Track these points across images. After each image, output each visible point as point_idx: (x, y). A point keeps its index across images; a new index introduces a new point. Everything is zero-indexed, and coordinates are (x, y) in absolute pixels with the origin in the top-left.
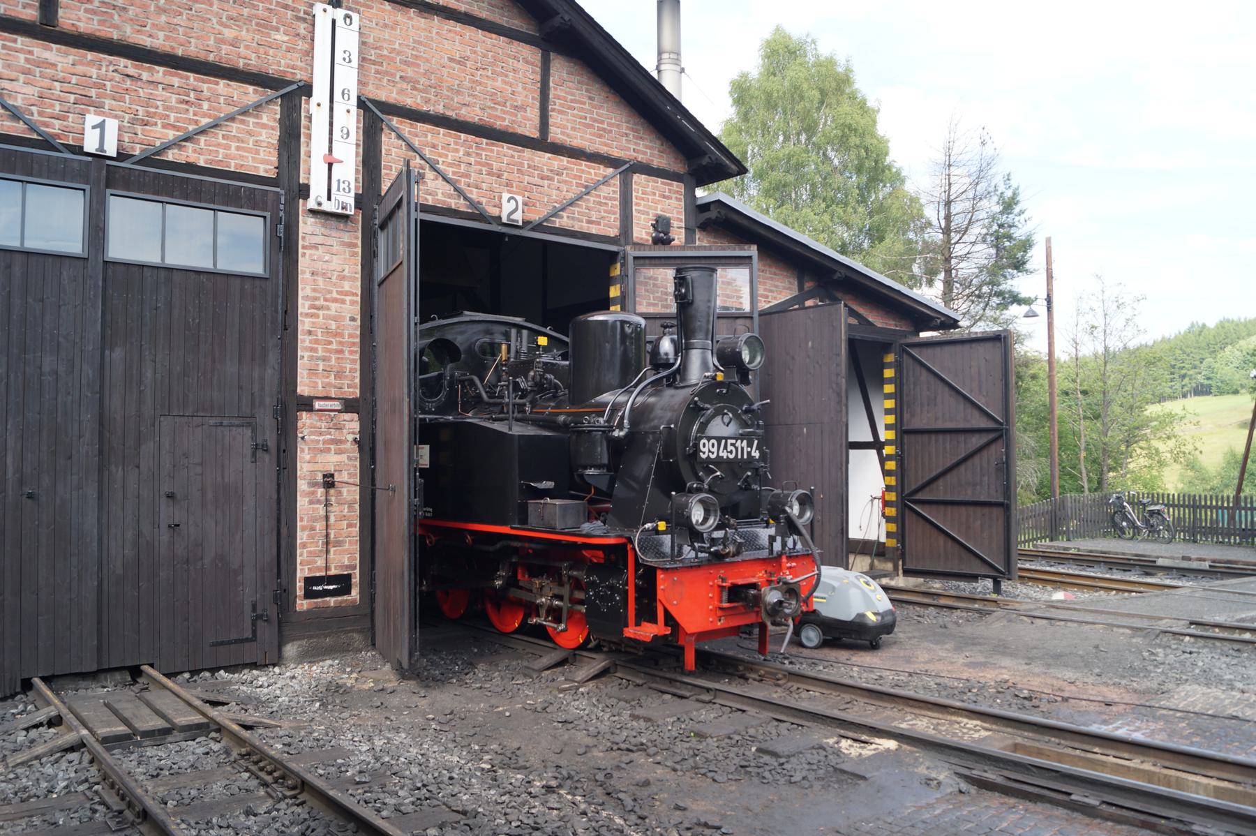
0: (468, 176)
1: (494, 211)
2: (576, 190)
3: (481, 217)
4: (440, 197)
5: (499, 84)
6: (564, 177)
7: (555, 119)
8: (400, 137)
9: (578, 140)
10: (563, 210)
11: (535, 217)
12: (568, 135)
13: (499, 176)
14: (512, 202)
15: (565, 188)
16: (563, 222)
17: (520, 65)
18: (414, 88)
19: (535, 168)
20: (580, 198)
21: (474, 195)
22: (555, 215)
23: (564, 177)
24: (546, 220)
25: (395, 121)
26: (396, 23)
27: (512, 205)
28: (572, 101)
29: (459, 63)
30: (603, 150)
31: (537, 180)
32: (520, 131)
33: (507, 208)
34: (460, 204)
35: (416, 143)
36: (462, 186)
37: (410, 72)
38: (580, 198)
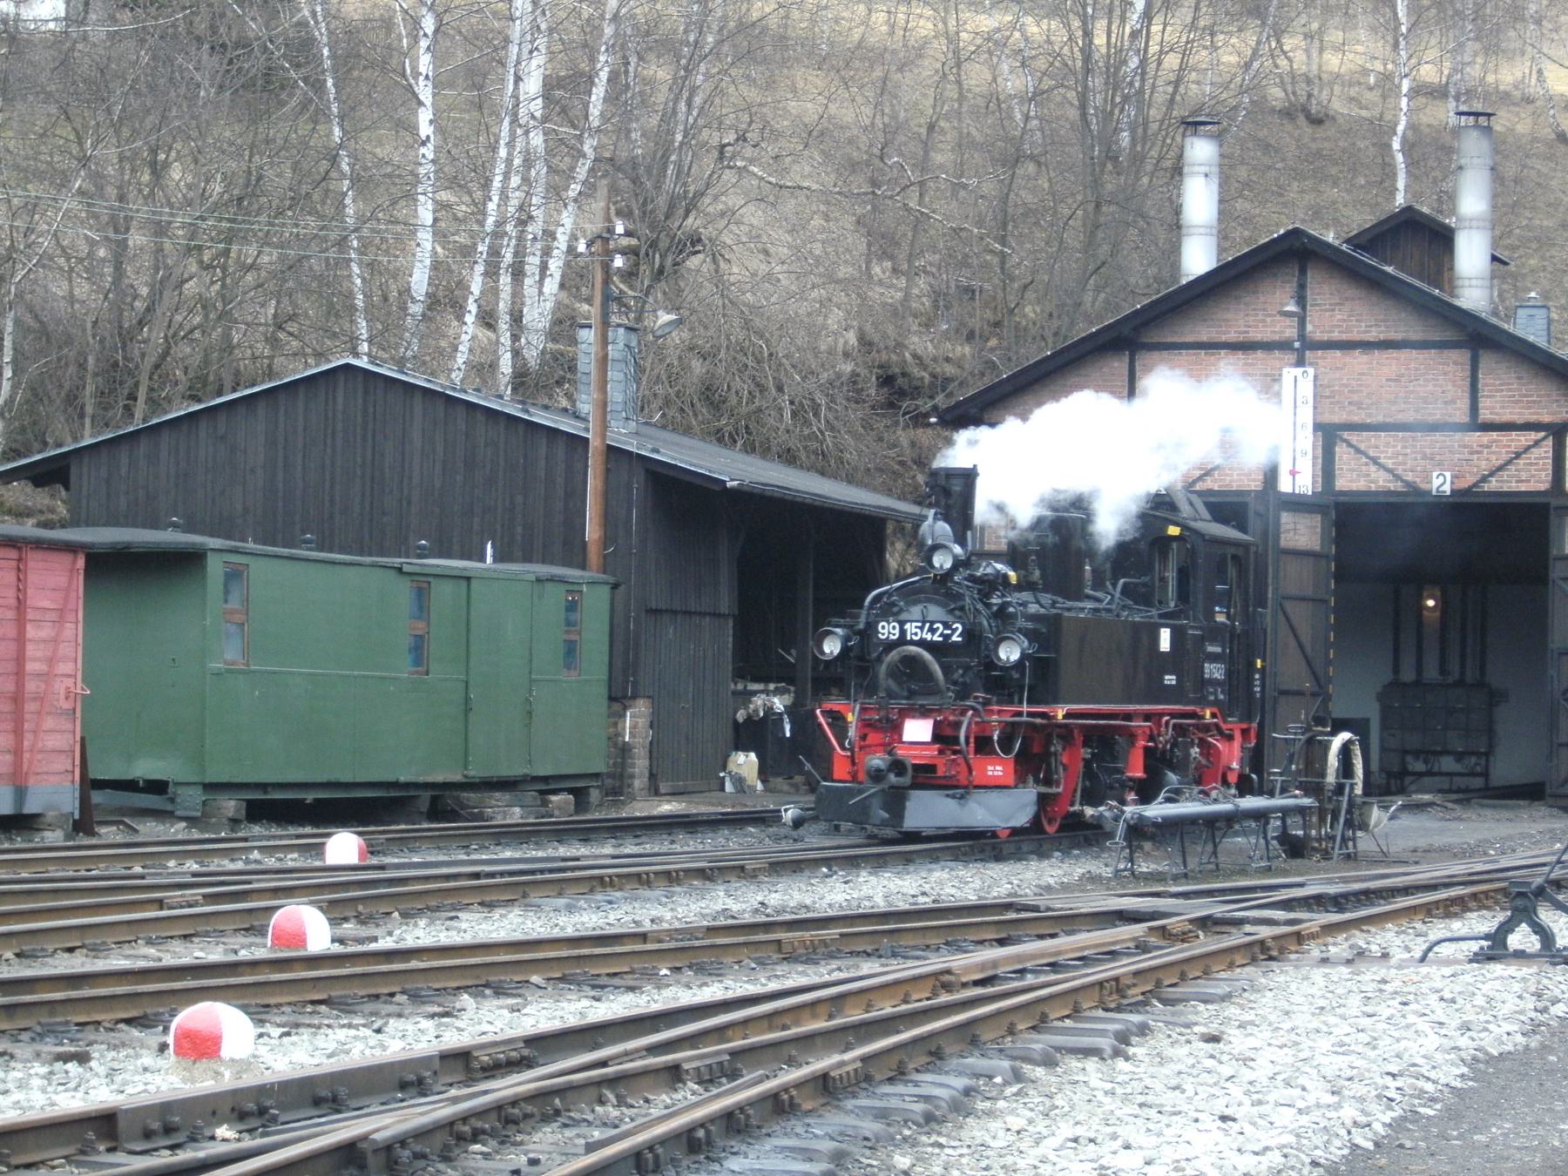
0: (1405, 464)
1: (1424, 486)
2: (1505, 457)
3: (1414, 490)
4: (1381, 483)
5: (1430, 388)
6: (1494, 449)
7: (1484, 403)
8: (1350, 445)
9: (1507, 416)
10: (1492, 474)
11: (1463, 484)
12: (1497, 414)
13: (1432, 459)
14: (1441, 478)
15: (1494, 457)
16: (1493, 485)
17: (1451, 368)
18: (1359, 408)
19: (1465, 447)
20: (1509, 462)
21: (1409, 477)
22: (1484, 479)
23: (1494, 449)
24: (1475, 485)
25: (1346, 435)
26: (1345, 364)
27: (1441, 479)
28: (1501, 385)
29: (1395, 380)
30: (1533, 418)
31: (1467, 456)
32: (1450, 420)
33: (1436, 482)
34: (1397, 486)
35: (1362, 447)
36: (1400, 472)
37: (1355, 398)
38: (1509, 462)
